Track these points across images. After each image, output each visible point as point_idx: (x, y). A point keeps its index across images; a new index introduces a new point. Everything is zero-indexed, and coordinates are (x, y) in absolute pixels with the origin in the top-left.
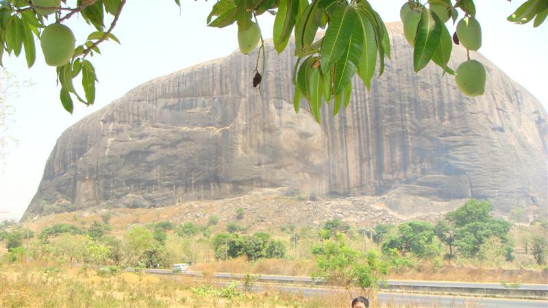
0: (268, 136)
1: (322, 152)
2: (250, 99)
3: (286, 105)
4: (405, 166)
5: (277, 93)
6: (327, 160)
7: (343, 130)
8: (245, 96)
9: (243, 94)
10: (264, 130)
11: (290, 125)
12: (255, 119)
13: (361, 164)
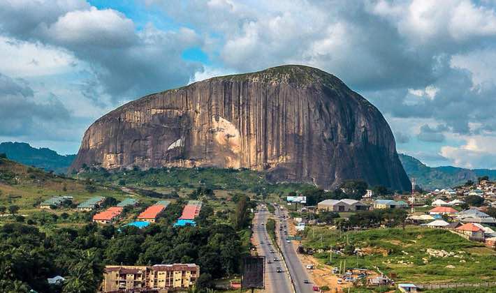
4: (278, 156)
13: (257, 154)
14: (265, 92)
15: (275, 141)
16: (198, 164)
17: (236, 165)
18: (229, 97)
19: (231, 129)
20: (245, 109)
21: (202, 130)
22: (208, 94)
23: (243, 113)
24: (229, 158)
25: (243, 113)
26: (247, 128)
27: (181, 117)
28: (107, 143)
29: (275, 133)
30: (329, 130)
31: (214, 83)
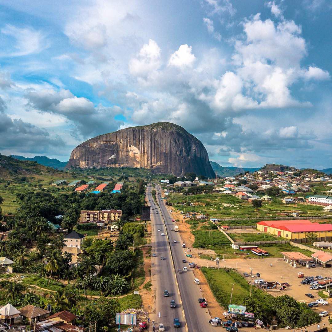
4: (157, 162)
13: (147, 162)
14: (151, 134)
15: (156, 156)
16: (122, 166)
17: (138, 166)
18: (135, 136)
19: (136, 150)
20: (142, 142)
21: (123, 151)
22: (126, 135)
23: (141, 143)
24: (135, 163)
25: (141, 143)
26: (143, 150)
27: (114, 145)
28: (81, 157)
29: (156, 152)
30: (179, 151)
31: (129, 130)
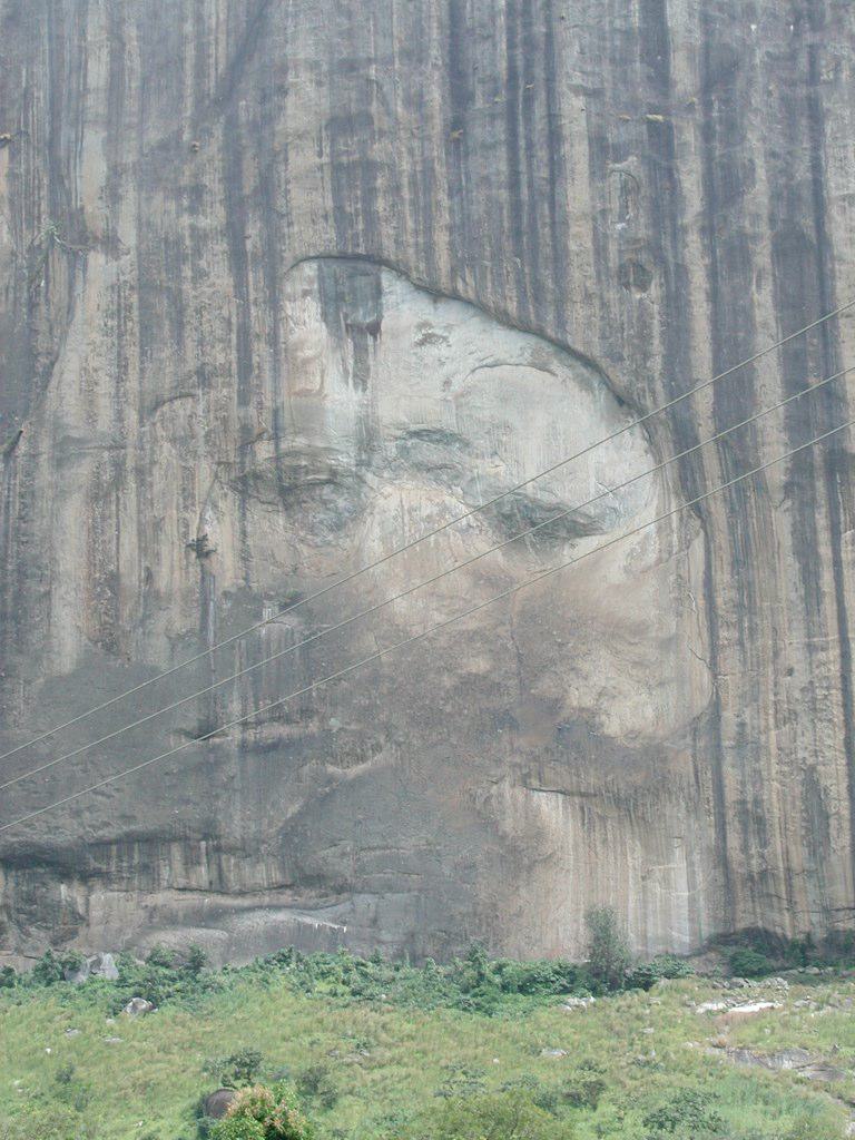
0: (272, 527)
1: (668, 644)
2: (143, 257)
3: (403, 309)
5: (341, 218)
6: (702, 702)
7: (820, 485)
8: (111, 244)
9: (98, 225)
10: (245, 485)
11: (434, 448)
12: (182, 408)
23: (725, 187)
25: (725, 187)
26: (794, 384)
